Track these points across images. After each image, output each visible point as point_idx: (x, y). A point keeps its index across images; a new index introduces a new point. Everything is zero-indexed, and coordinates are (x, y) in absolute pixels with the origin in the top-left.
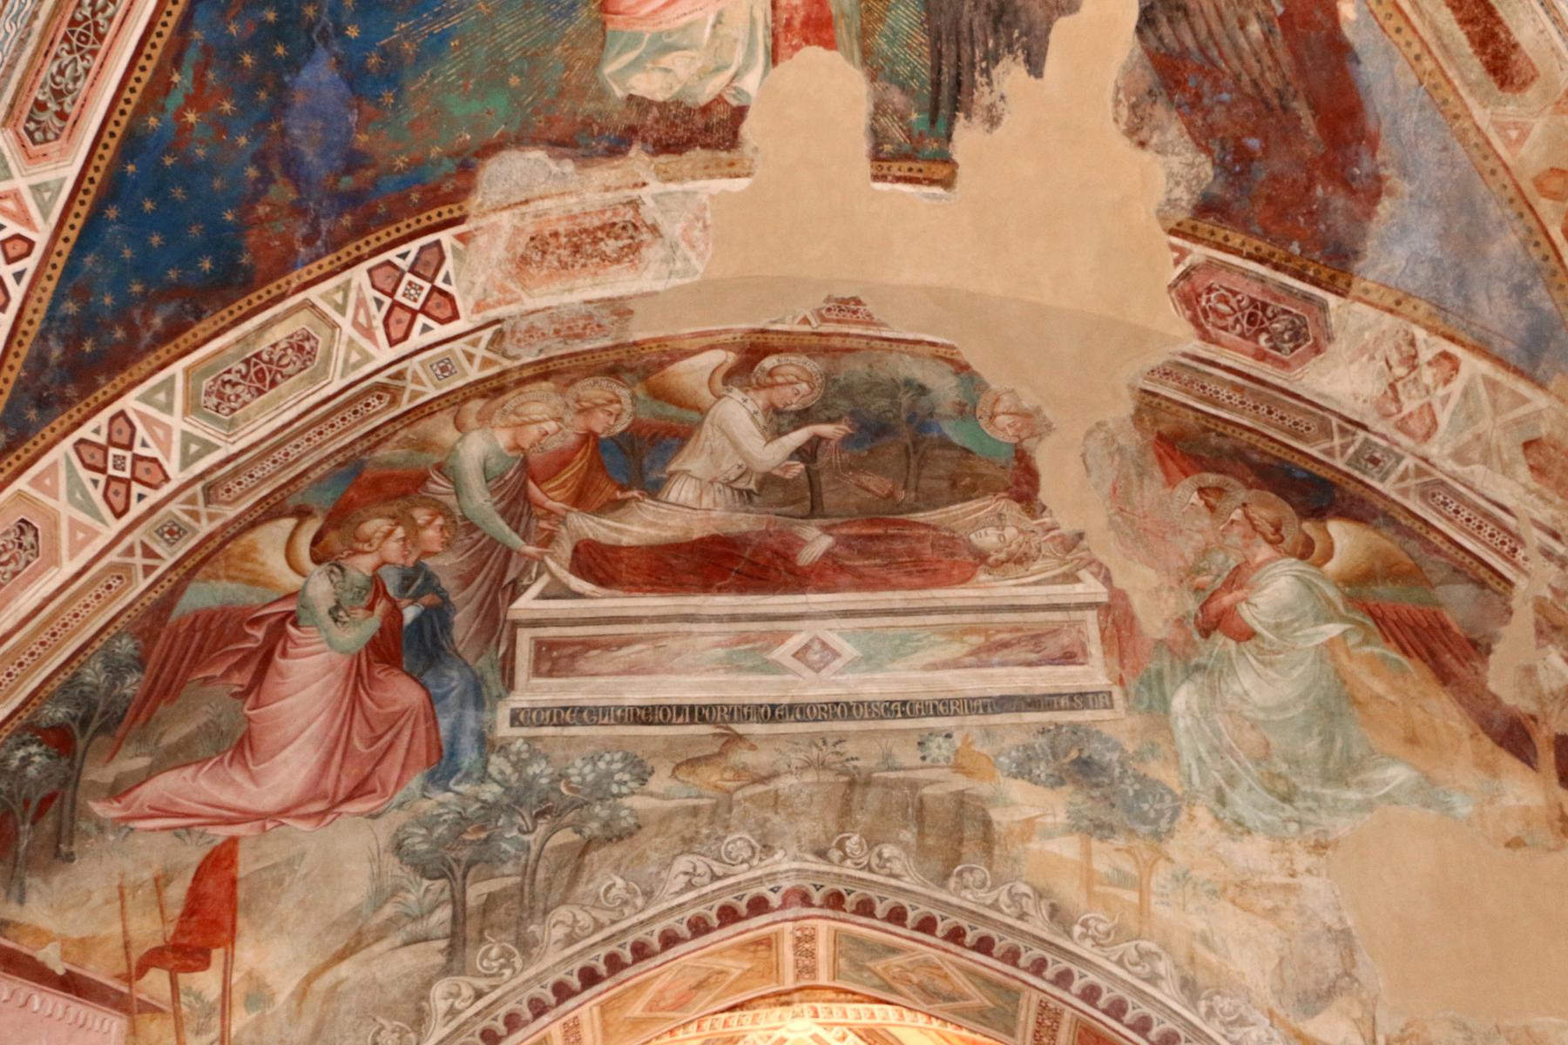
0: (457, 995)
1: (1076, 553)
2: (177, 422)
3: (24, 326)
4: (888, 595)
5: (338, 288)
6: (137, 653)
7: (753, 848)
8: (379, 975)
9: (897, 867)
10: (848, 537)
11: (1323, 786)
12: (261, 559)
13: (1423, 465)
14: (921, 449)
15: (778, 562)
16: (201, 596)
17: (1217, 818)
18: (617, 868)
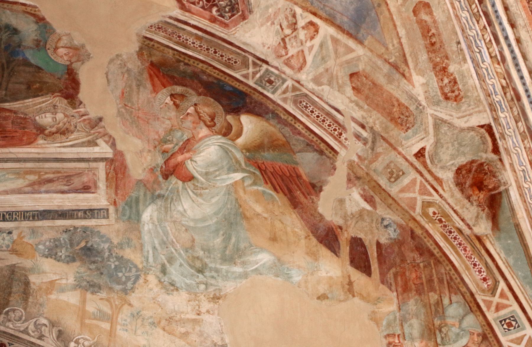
1: (97, 129)
11: (221, 264)
13: (297, 85)
17: (160, 281)
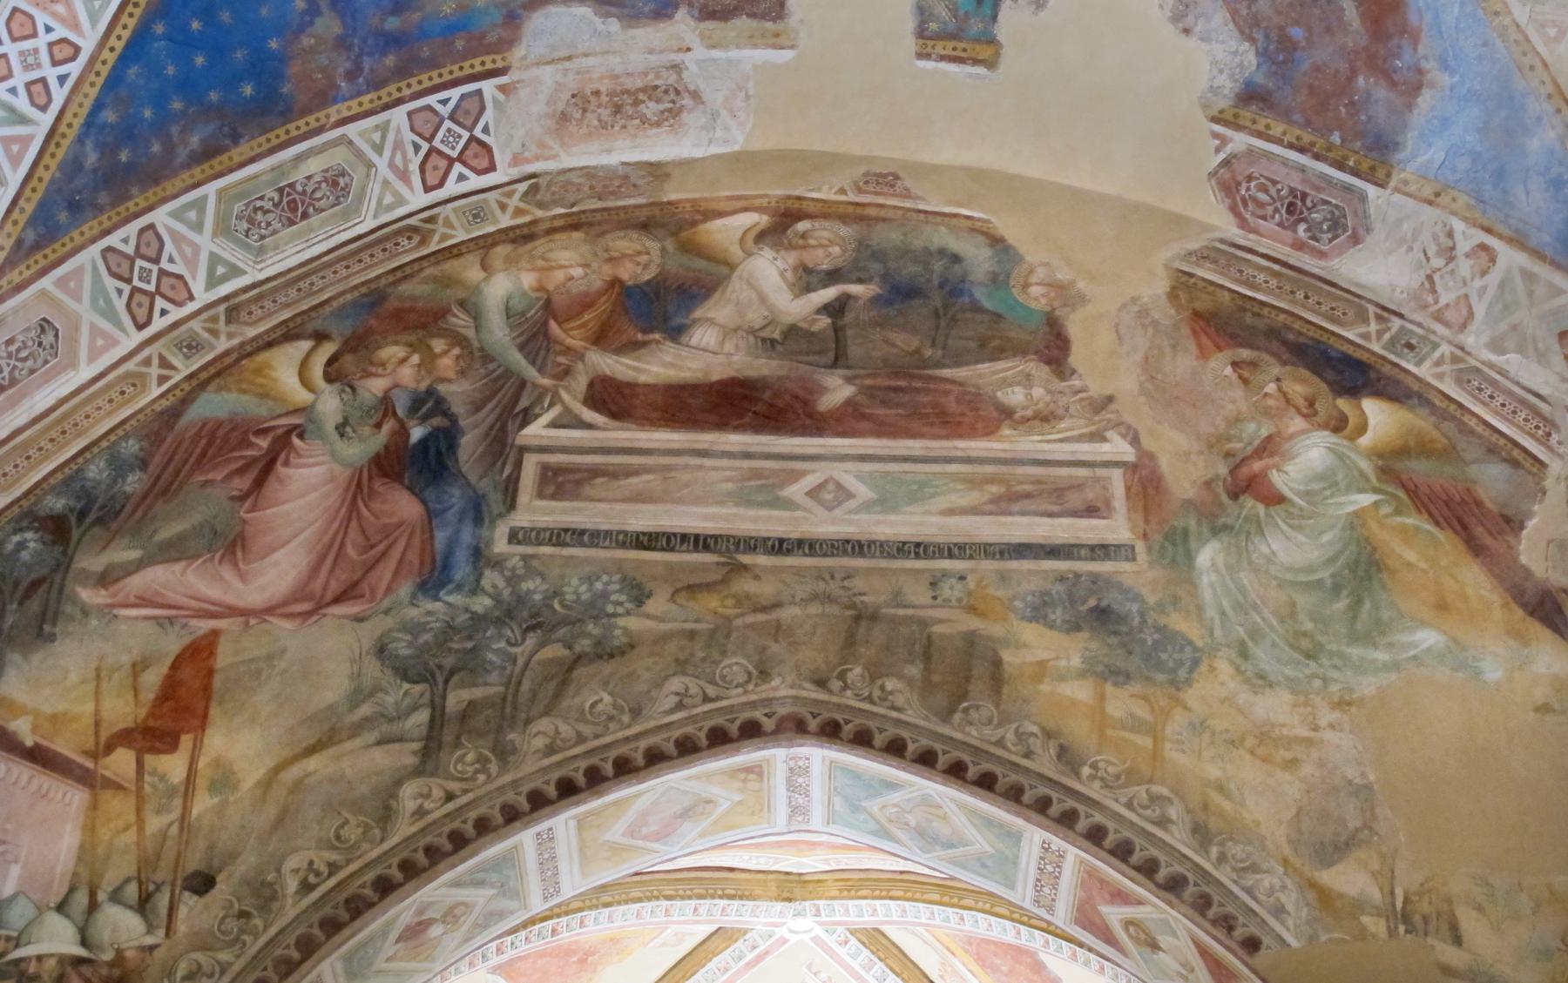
0: (427, 796)
1: (1106, 415)
2: (206, 242)
3: (63, 128)
4: (910, 443)
5: (377, 126)
6: (141, 454)
7: (749, 674)
8: (348, 771)
9: (900, 701)
10: (871, 388)
11: (1348, 645)
12: (274, 374)
13: (1459, 353)
14: (951, 313)
15: (797, 405)
16: (214, 405)
17: (1238, 669)
18: (605, 684)
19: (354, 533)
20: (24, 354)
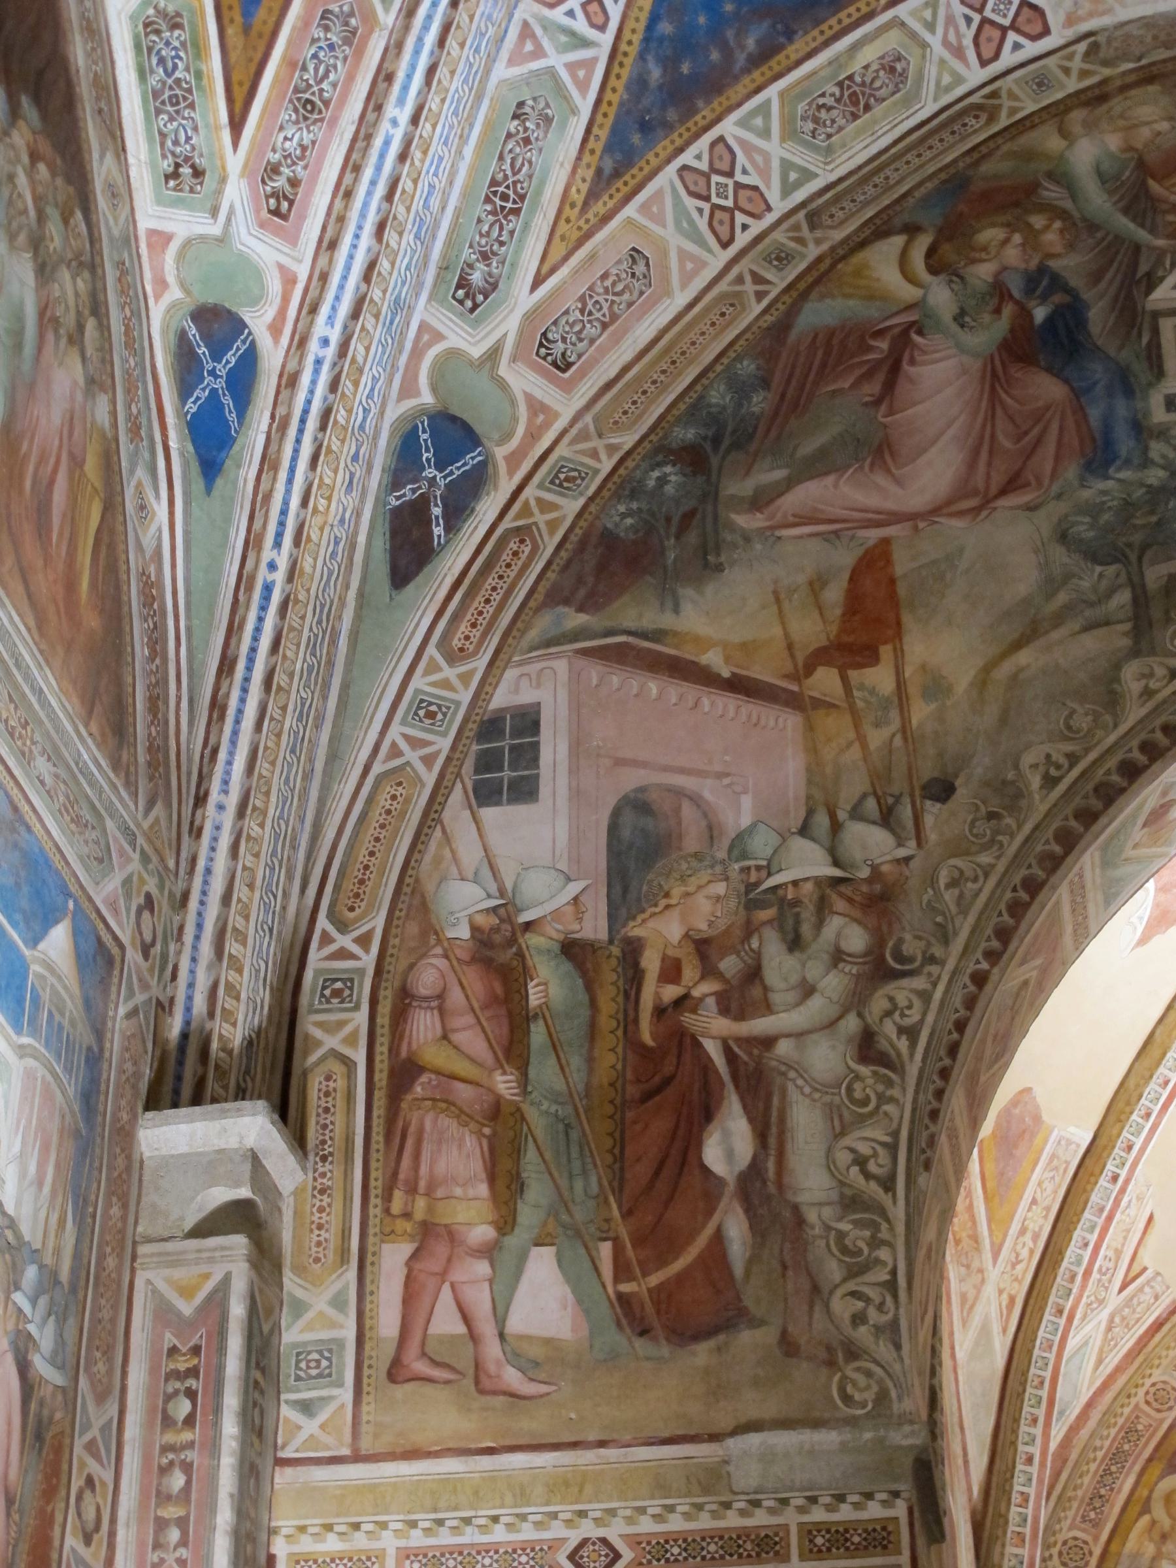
0: (1151, 675)
2: (775, 149)
3: (623, 47)
19: (1001, 423)
20: (619, 287)
